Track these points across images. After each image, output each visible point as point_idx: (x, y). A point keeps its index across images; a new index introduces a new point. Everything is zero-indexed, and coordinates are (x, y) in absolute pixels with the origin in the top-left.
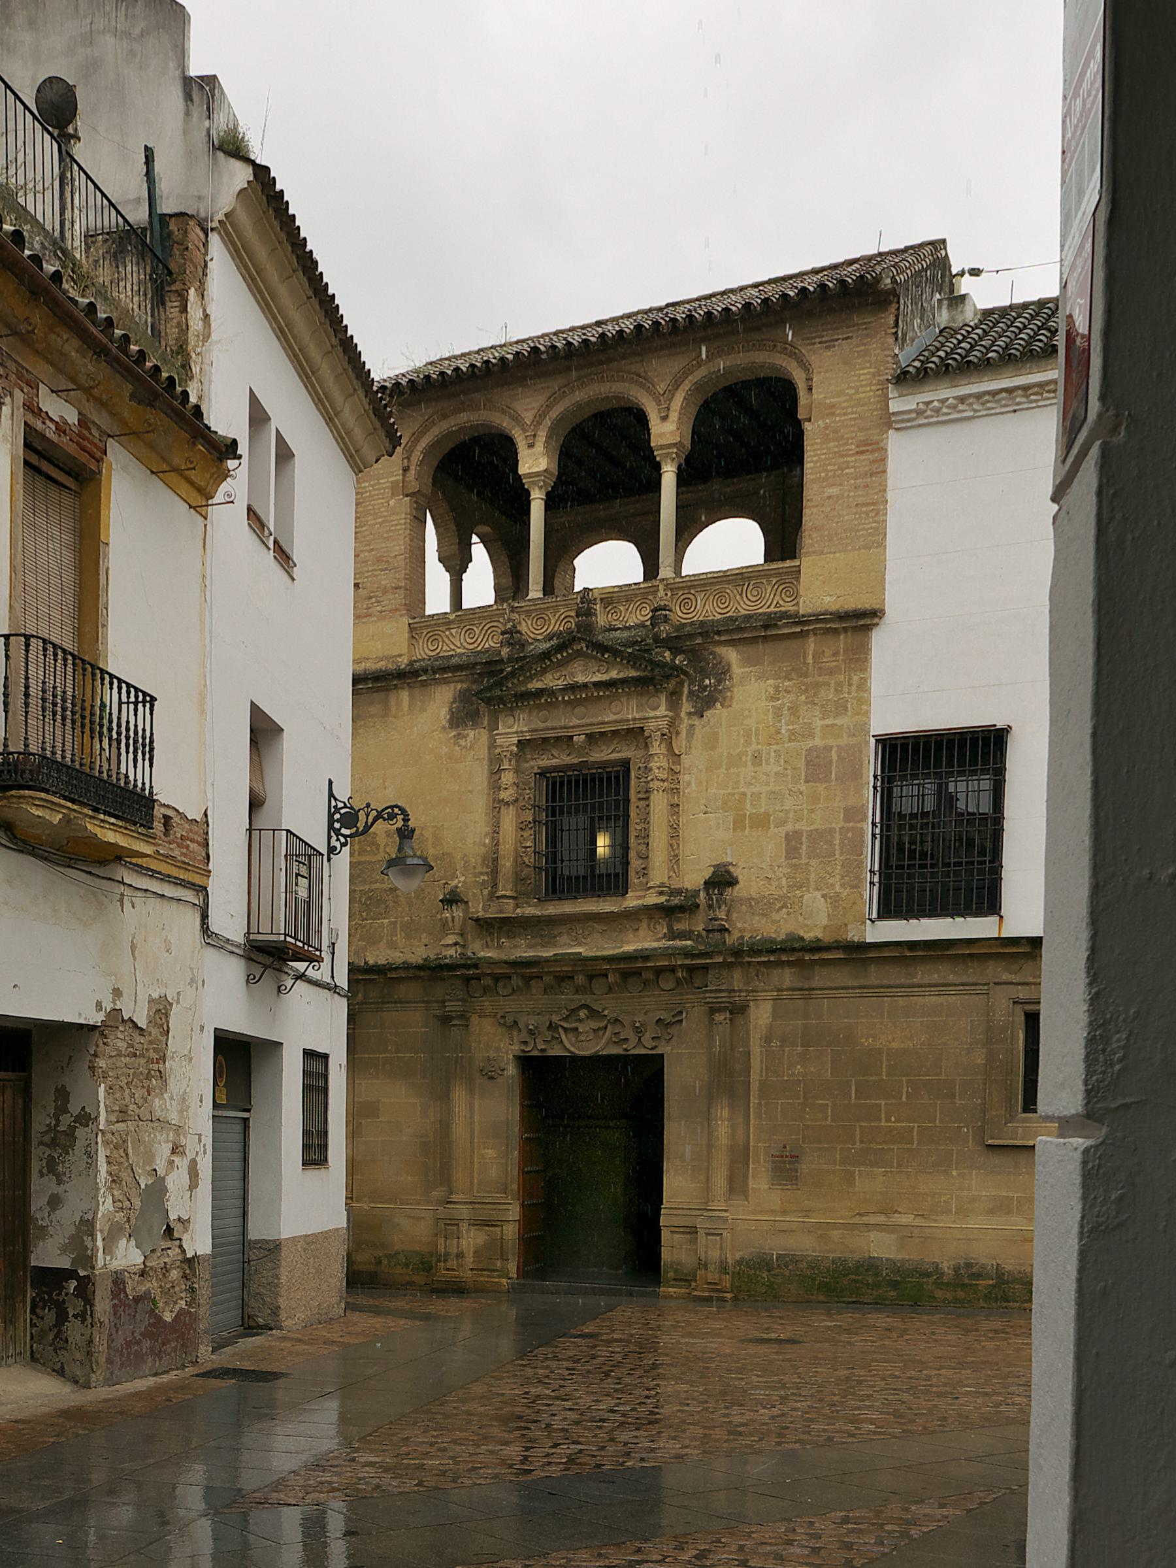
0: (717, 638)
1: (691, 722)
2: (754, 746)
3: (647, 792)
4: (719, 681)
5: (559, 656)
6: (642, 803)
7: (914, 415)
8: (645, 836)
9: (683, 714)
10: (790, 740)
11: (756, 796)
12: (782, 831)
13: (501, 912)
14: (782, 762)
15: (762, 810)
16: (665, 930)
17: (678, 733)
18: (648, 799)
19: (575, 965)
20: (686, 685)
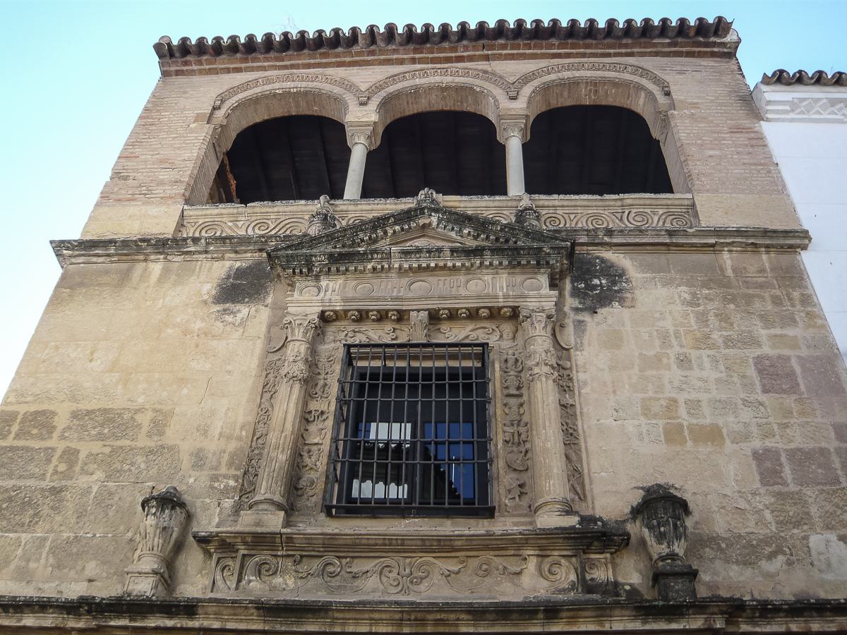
0: (607, 239)
1: (580, 317)
2: (677, 349)
3: (519, 388)
4: (614, 283)
5: (397, 228)
6: (513, 401)
7: (787, 108)
8: (521, 442)
9: (566, 309)
10: (727, 347)
11: (694, 405)
12: (747, 448)
13: (257, 524)
14: (722, 368)
15: (708, 421)
16: (573, 577)
17: (562, 326)
18: (520, 396)
19: (400, 622)
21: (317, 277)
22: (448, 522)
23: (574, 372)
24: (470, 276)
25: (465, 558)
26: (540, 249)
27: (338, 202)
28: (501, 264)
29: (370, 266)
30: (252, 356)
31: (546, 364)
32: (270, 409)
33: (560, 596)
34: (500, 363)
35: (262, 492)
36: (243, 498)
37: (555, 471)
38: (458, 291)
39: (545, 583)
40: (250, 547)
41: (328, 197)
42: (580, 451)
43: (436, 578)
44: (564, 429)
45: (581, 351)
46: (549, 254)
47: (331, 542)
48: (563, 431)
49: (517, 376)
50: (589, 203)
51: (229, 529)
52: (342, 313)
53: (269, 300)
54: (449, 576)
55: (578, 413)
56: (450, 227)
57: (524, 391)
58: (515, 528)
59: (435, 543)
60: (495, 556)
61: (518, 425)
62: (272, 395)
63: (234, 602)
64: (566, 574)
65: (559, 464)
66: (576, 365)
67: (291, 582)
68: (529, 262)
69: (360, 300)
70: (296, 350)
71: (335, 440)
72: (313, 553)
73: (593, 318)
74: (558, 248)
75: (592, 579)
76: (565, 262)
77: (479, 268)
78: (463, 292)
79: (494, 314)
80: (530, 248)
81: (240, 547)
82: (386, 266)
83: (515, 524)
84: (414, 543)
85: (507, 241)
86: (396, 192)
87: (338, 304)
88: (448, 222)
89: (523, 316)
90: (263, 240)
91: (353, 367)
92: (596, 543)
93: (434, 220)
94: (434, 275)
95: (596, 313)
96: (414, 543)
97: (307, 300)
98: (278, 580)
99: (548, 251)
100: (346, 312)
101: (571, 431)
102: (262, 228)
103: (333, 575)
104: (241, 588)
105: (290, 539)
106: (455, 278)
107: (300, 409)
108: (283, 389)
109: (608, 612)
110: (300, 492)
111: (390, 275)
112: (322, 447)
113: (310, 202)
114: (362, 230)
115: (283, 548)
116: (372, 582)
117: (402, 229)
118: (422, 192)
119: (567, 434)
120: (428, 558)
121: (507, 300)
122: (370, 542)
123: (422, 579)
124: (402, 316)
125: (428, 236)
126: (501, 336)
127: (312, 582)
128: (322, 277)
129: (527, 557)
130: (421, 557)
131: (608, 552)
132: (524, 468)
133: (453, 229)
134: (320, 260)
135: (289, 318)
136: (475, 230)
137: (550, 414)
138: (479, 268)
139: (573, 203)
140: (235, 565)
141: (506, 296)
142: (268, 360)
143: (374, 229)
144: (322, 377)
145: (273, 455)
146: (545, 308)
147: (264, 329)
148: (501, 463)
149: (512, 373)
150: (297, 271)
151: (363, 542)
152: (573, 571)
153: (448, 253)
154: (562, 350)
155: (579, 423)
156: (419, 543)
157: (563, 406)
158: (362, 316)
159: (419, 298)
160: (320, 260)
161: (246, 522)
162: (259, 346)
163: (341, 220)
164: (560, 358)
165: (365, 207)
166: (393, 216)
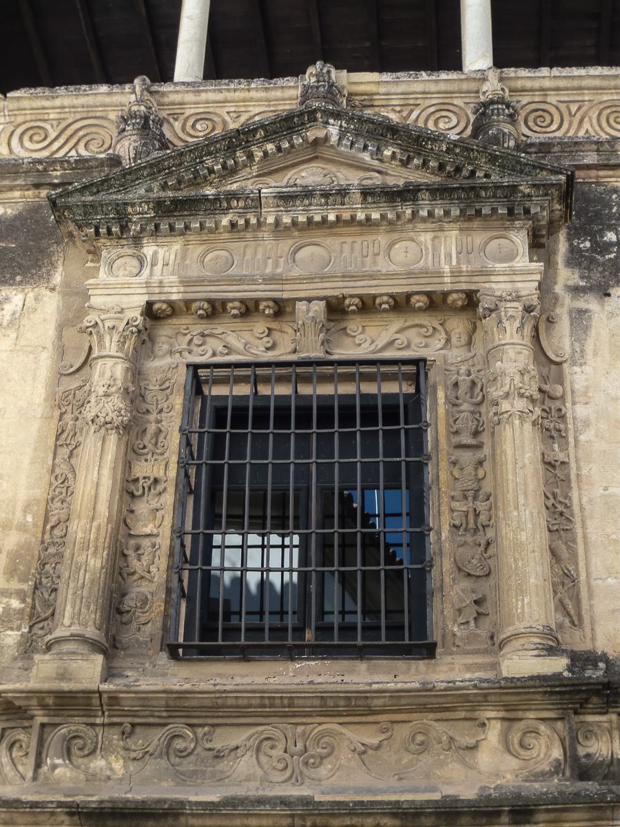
1: (581, 304)
3: (476, 433)
5: (270, 147)
6: (467, 457)
8: (479, 527)
9: (559, 289)
16: (557, 753)
17: (550, 321)
18: (479, 447)
20: (562, 237)
21: (137, 241)
22: (362, 666)
23: (569, 405)
24: (396, 235)
25: (389, 724)
26: (514, 188)
27: (166, 88)
28: (447, 213)
29: (225, 221)
30: (34, 380)
31: (521, 396)
32: (70, 476)
33: (537, 785)
34: (446, 388)
35: (67, 621)
36: (35, 630)
37: (532, 580)
38: (375, 263)
39: (513, 763)
40: (52, 713)
41: (148, 81)
42: (574, 541)
43: (345, 756)
44: (549, 504)
45: (581, 365)
46: (529, 195)
47: (178, 703)
48: (547, 508)
49: (473, 413)
50: (605, 83)
51: (18, 686)
52: (182, 305)
53: (57, 278)
54: (364, 752)
55: (573, 477)
56: (360, 145)
57: (485, 438)
58: (468, 676)
59: (342, 703)
60: (437, 720)
61: (475, 498)
62: (71, 452)
63: (34, 805)
64: (547, 749)
65: (539, 569)
66: (573, 392)
67: (118, 765)
68: (494, 210)
69: (212, 282)
70: (108, 374)
71: (178, 533)
72: (151, 720)
73: (603, 306)
74: (543, 185)
75: (588, 756)
76: (558, 207)
77: (410, 221)
78: (383, 266)
79: (436, 303)
80: (497, 187)
81: (36, 712)
82: (253, 221)
83: (468, 668)
84: (308, 702)
85: (458, 170)
86: (273, 66)
87: (174, 290)
88: (357, 135)
89: (485, 309)
90: (40, 167)
91: (204, 399)
92: (595, 700)
93: (333, 131)
94: (335, 235)
95: (609, 295)
96: (308, 702)
97: (123, 281)
98: (98, 763)
99: (527, 191)
100: (188, 303)
101: (560, 508)
102: (36, 138)
103: (183, 754)
104: (41, 778)
105: (114, 699)
106: (370, 238)
107: (119, 478)
108: (90, 442)
109: (608, 813)
110: (125, 618)
111: (260, 235)
112: (158, 540)
113: (116, 89)
114: (210, 154)
115: (103, 713)
116: (244, 765)
117: (279, 149)
118: (311, 70)
119: (554, 513)
120: (332, 725)
121: (457, 279)
122: (240, 702)
123: (322, 758)
124: (281, 309)
125: (323, 158)
126: (448, 341)
127: (151, 766)
128: (145, 241)
129: (486, 721)
130: (320, 724)
131: (613, 712)
132: (484, 571)
133: (365, 147)
134: (140, 213)
135: (92, 318)
136: (404, 150)
137: (525, 484)
138: (410, 221)
139: (575, 83)
140: (29, 740)
141: (456, 273)
142: (62, 389)
143: (231, 149)
144: (152, 417)
145: (80, 559)
146: (523, 293)
147: (51, 332)
148: (447, 565)
149: (465, 407)
150: (103, 231)
151: (229, 702)
152: (557, 744)
153: (358, 197)
154: (548, 366)
155: (575, 494)
156: (317, 702)
157: (549, 464)
158: (216, 310)
159: (310, 279)
160: (140, 213)
161: (43, 673)
162: (45, 363)
163: (171, 120)
164: (545, 379)
165: (212, 96)
166: (263, 126)
